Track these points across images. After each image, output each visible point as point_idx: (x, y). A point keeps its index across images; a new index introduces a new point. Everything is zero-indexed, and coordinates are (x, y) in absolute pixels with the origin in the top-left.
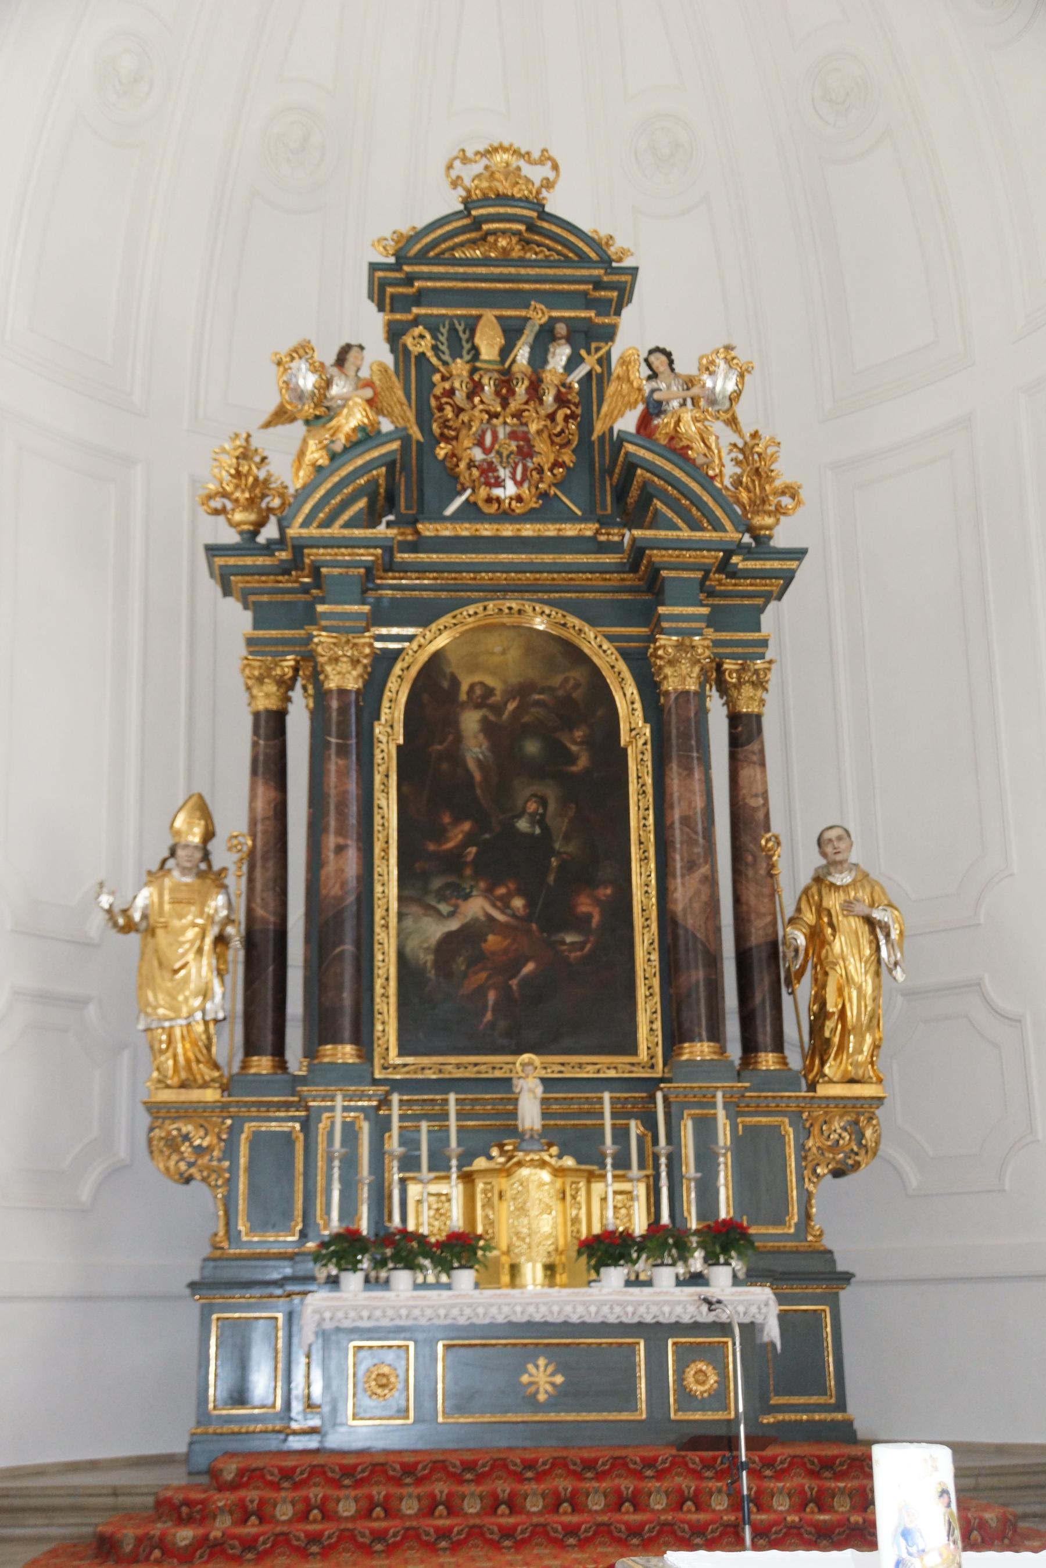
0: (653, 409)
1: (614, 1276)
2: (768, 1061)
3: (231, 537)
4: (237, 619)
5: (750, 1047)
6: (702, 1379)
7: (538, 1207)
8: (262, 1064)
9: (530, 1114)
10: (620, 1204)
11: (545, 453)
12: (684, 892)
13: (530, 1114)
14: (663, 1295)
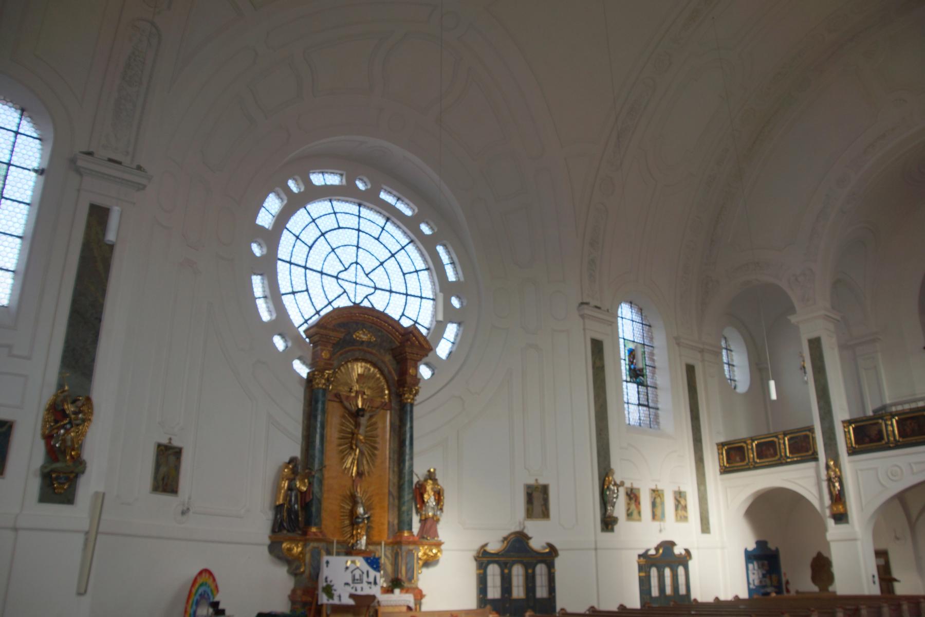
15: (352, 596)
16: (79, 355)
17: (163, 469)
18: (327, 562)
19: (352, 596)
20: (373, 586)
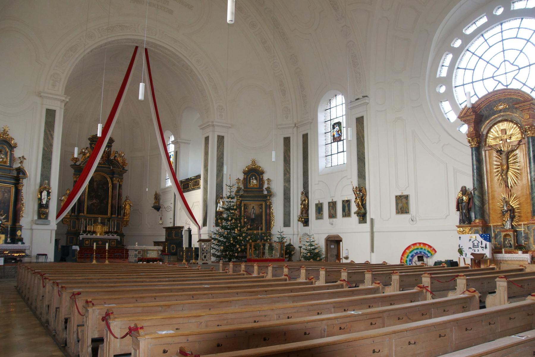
0: (115, 157)
1: (106, 235)
2: (119, 217)
3: (73, 164)
4: (72, 171)
5: (118, 215)
6: (113, 243)
7: (99, 228)
8: (73, 214)
9: (99, 221)
10: (106, 229)
11: (105, 158)
12: (114, 202)
13: (99, 221)
14: (111, 237)
15: (472, 254)
16: (361, 174)
17: (400, 205)
18: (460, 238)
19: (472, 254)
20: (484, 249)
